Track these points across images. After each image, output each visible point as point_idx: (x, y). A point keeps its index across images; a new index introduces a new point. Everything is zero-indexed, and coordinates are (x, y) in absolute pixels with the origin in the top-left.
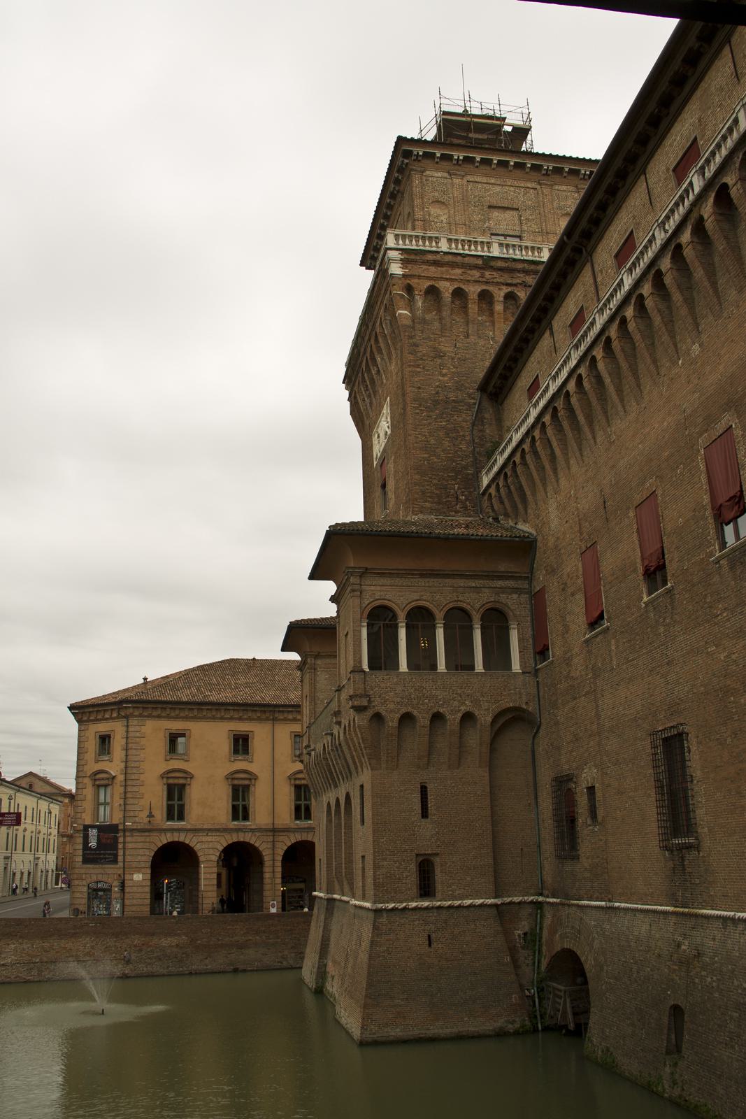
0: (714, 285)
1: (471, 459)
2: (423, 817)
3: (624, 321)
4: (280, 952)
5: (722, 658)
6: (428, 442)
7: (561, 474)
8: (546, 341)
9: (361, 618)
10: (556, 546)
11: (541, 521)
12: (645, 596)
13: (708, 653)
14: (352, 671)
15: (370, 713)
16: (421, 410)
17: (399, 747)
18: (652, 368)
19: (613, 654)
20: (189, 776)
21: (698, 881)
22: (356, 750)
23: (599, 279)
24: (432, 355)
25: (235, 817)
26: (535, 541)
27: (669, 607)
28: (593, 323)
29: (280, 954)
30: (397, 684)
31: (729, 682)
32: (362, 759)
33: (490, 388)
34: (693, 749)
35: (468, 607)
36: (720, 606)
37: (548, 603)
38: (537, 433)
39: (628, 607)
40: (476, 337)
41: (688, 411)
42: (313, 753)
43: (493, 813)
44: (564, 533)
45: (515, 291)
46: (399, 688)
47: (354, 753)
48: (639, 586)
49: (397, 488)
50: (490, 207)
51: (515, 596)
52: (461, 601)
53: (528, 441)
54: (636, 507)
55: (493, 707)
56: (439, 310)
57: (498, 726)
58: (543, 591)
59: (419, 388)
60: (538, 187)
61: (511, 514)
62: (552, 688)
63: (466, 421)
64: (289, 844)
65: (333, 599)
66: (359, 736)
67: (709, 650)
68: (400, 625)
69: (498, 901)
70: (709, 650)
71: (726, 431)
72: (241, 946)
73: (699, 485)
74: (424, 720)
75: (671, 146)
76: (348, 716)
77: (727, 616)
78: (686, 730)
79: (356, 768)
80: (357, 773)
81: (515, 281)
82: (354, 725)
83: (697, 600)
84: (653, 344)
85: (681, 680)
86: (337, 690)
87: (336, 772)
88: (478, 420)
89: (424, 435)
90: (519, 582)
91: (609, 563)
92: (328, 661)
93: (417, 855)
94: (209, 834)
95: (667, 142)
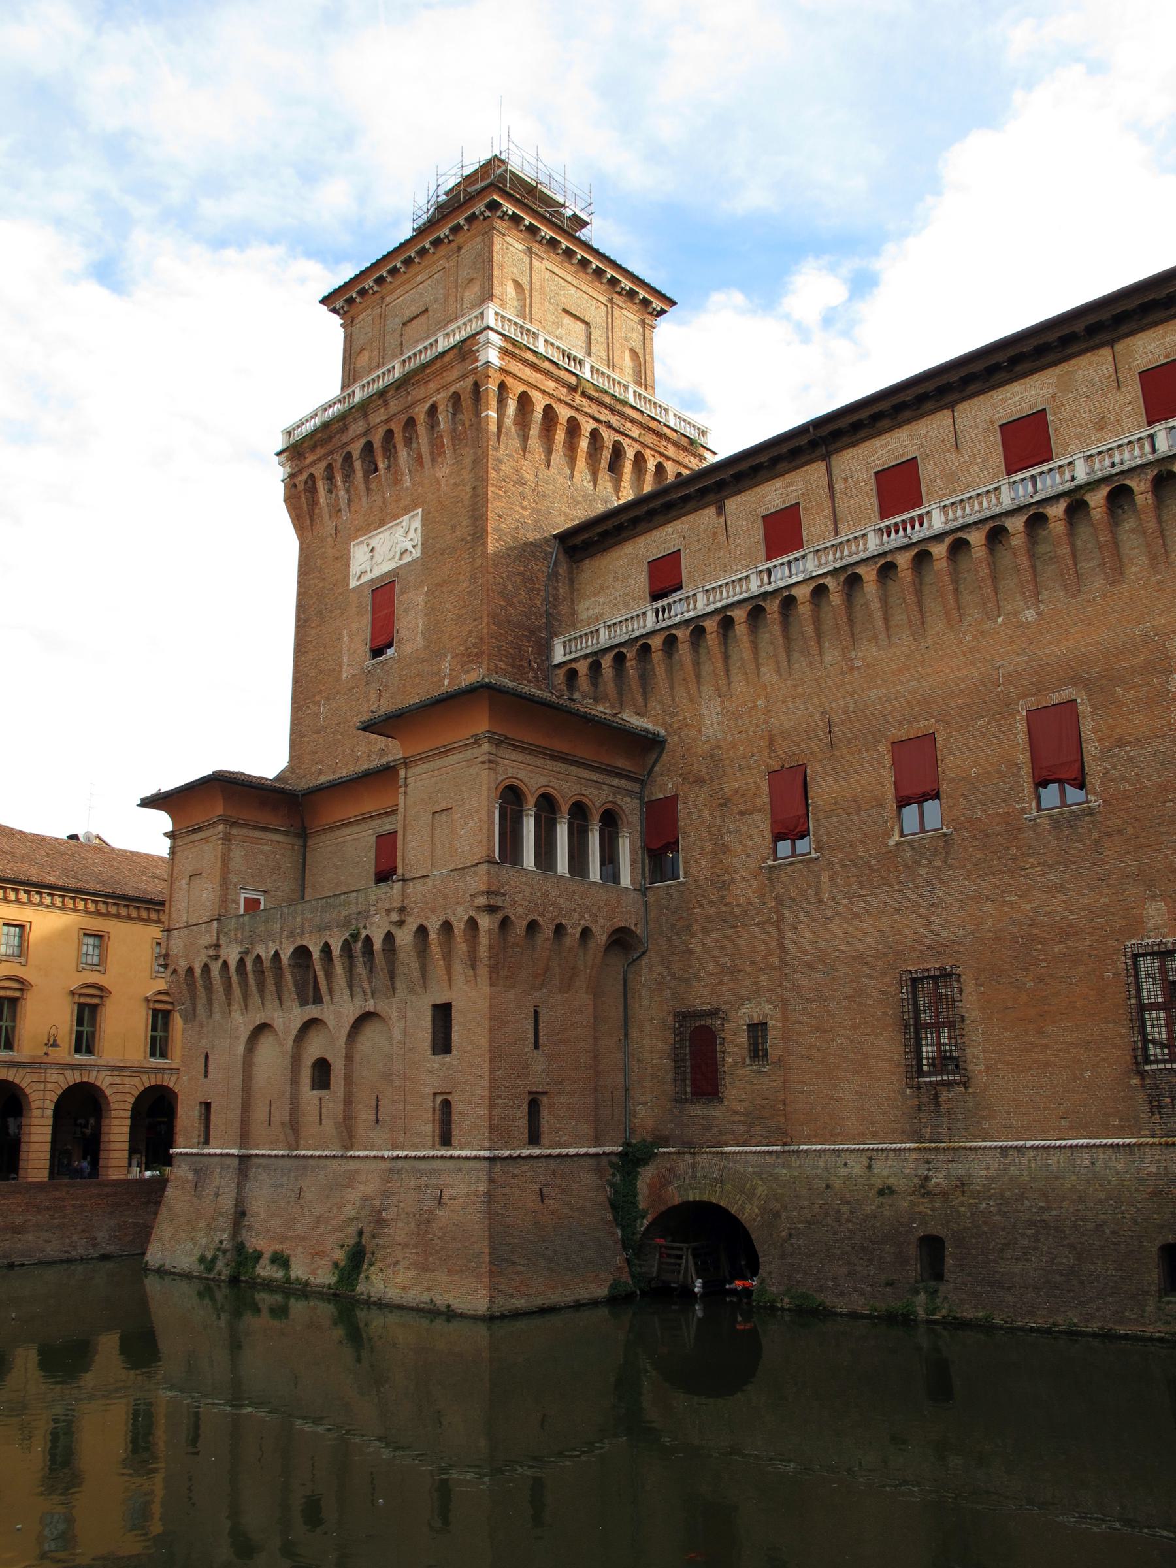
1: (545, 620)
4: (68, 1237)
6: (506, 587)
21: (960, 1116)
23: (839, 486)
24: (514, 479)
29: (67, 1241)
35: (590, 804)
36: (1031, 860)
46: (528, 890)
50: (565, 311)
51: (628, 799)
52: (584, 795)
59: (499, 516)
60: (609, 305)
63: (542, 572)
67: (1008, 899)
69: (600, 1150)
70: (1008, 899)
72: (19, 1230)
74: (548, 931)
75: (1003, 401)
81: (602, 418)
88: (553, 576)
89: (503, 578)
90: (633, 784)
92: (244, 831)
93: (530, 1093)
95: (998, 395)
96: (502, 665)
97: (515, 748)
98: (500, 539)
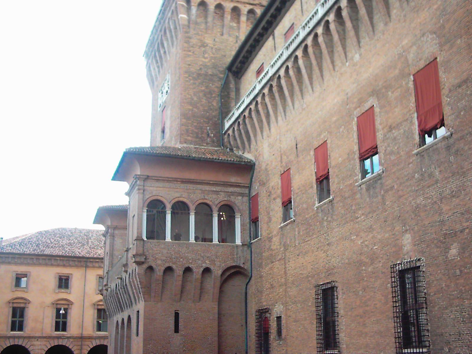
0: (371, 18)
2: (175, 332)
3: (316, 36)
5: (360, 243)
6: (193, 99)
7: (272, 125)
8: (269, 43)
9: (143, 206)
10: (266, 169)
11: (258, 153)
12: (317, 202)
13: (351, 240)
14: (136, 240)
15: (145, 266)
16: (190, 79)
17: (163, 287)
18: (331, 66)
19: (296, 237)
20: (27, 302)
22: (135, 289)
23: (305, 7)
25: (57, 329)
26: (254, 164)
27: (331, 211)
28: (297, 35)
30: (164, 248)
31: (362, 258)
32: (139, 294)
33: (234, 69)
34: (340, 297)
35: (210, 203)
36: (360, 212)
37: (259, 203)
38: (259, 99)
39: (307, 209)
40: (228, 36)
41: (350, 94)
42: (109, 289)
43: (219, 331)
44: (272, 162)
45: (255, 9)
46: (165, 251)
47: (134, 291)
48: (314, 196)
49: (171, 126)
51: (240, 198)
52: (206, 199)
53: (254, 103)
54: (315, 149)
55: (223, 265)
56: (206, 17)
57: (225, 277)
58: (257, 195)
59: (189, 65)
61: (241, 147)
62: (259, 255)
64: (92, 347)
65: (128, 194)
66: (138, 280)
67: (352, 238)
68: (167, 212)
71: (370, 108)
73: (352, 139)
74: (179, 271)
76: (132, 267)
77: (364, 218)
78: (336, 285)
79: (135, 300)
80: (136, 303)
82: (135, 273)
83: (347, 208)
84: (332, 51)
85: (335, 255)
86: (126, 251)
87: (123, 302)
89: (191, 95)
91: (297, 181)
94: (39, 340)
96: (189, 138)
97: (157, 180)
98: (189, 76)
